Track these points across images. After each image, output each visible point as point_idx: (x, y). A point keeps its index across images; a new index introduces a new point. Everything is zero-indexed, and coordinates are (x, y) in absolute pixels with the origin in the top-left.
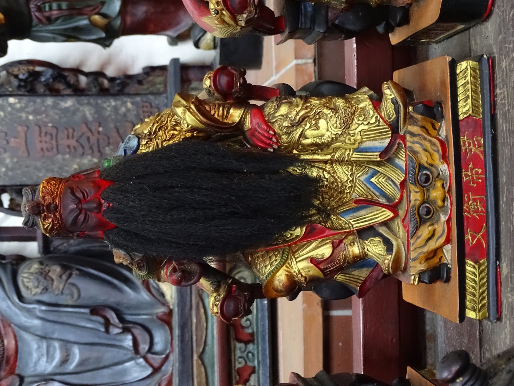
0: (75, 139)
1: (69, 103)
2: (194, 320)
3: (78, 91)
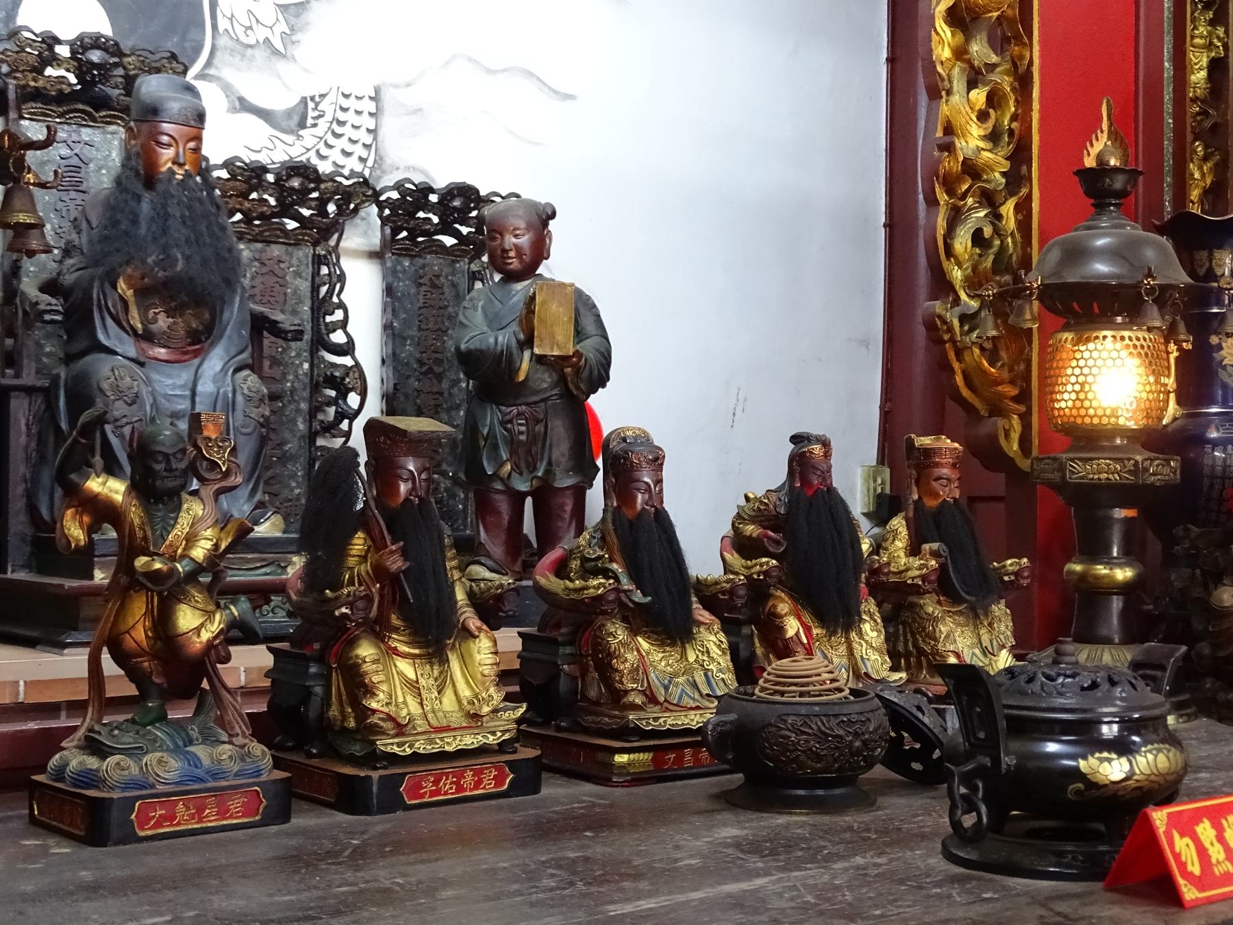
1: (301, 426)
2: (250, 556)
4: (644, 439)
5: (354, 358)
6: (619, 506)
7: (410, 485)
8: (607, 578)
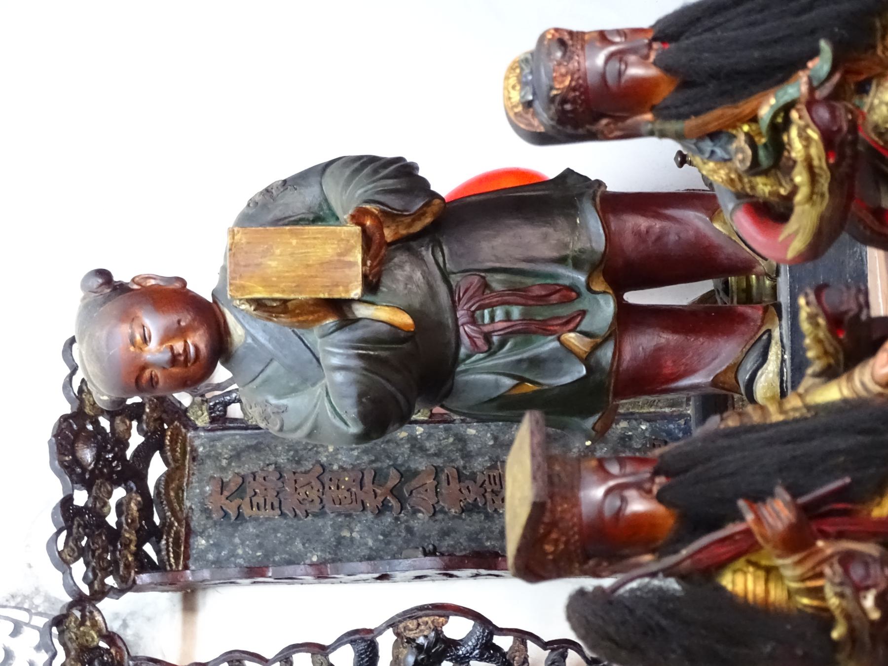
4: (528, 65)
5: (380, 631)
6: (653, 109)
7: (631, 494)
8: (788, 122)
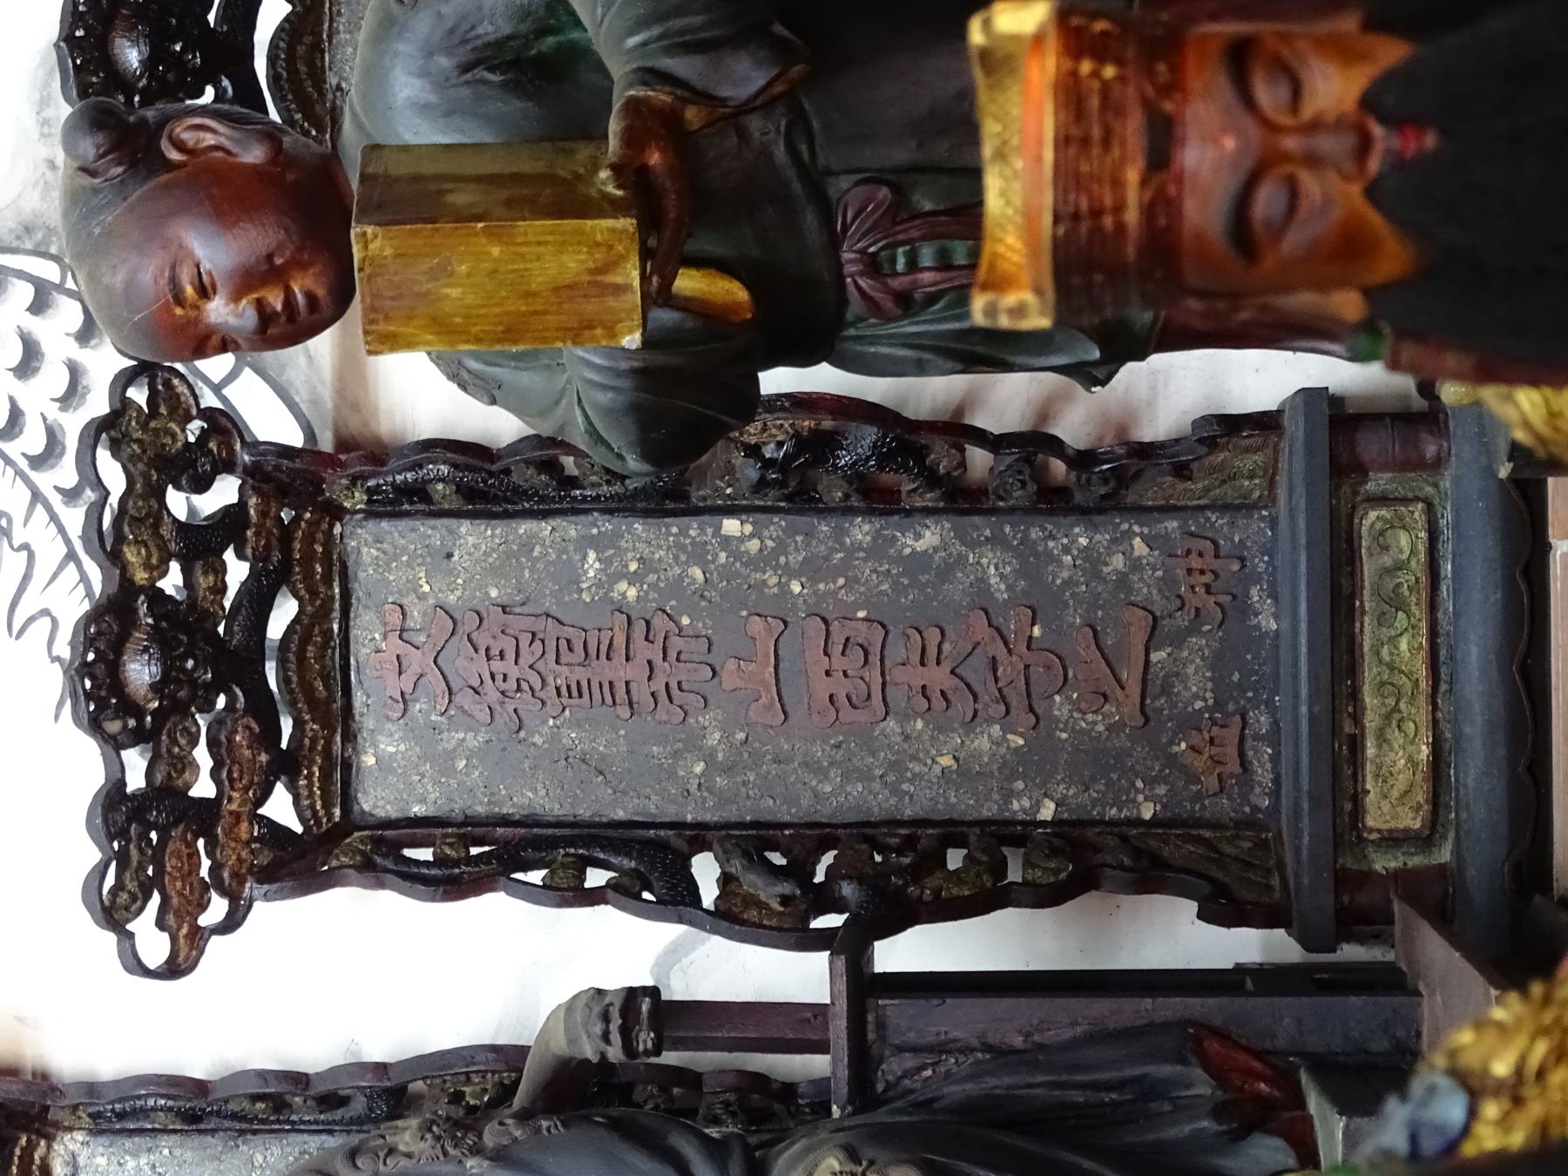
0: (947, 666)
1: (929, 538)
3: (962, 499)
